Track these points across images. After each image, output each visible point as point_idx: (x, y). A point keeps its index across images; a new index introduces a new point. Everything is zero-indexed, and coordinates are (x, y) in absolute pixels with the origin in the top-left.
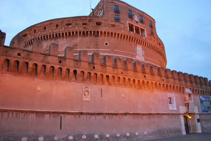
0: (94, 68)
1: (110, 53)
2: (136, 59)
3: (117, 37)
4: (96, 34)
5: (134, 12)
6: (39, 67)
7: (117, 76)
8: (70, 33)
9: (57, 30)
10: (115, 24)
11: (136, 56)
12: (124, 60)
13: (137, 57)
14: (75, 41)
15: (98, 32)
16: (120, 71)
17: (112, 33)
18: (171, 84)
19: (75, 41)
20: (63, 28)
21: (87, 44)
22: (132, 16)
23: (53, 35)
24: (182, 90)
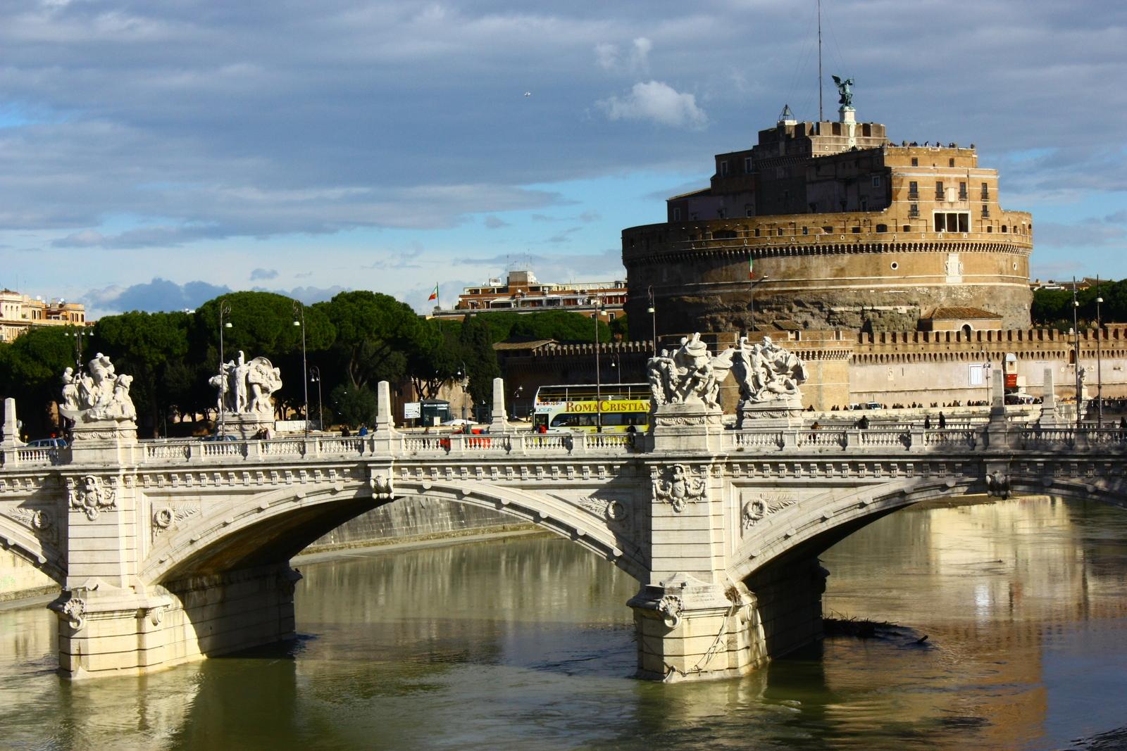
2: (945, 284)
4: (877, 248)
6: (857, 357)
14: (840, 261)
16: (921, 346)
17: (904, 245)
21: (861, 267)
23: (799, 248)
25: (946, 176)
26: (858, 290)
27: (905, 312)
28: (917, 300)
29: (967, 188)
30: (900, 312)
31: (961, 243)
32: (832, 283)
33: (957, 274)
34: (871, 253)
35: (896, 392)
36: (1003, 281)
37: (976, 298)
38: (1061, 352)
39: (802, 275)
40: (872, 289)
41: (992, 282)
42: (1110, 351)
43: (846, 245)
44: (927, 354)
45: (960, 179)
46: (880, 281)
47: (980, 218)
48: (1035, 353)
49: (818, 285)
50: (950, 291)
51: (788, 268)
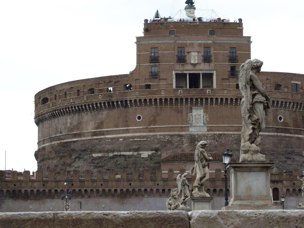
1: (143, 132)
2: (188, 133)
3: (154, 104)
4: (125, 104)
5: (189, 46)
7: (96, 189)
8: (93, 104)
10: (151, 84)
11: (190, 128)
12: (165, 139)
13: (191, 129)
14: (100, 116)
15: (126, 101)
17: (145, 100)
19: (101, 116)
20: (85, 97)
21: (115, 120)
22: (186, 56)
25: (188, 42)
26: (112, 139)
27: (147, 156)
28: (158, 146)
29: (212, 52)
30: (142, 156)
32: (95, 134)
33: (202, 125)
34: (121, 109)
37: (222, 145)
39: (78, 129)
40: (121, 138)
43: (102, 102)
44: (107, 190)
45: (204, 44)
46: (127, 131)
47: (227, 77)
49: (87, 137)
51: (71, 123)
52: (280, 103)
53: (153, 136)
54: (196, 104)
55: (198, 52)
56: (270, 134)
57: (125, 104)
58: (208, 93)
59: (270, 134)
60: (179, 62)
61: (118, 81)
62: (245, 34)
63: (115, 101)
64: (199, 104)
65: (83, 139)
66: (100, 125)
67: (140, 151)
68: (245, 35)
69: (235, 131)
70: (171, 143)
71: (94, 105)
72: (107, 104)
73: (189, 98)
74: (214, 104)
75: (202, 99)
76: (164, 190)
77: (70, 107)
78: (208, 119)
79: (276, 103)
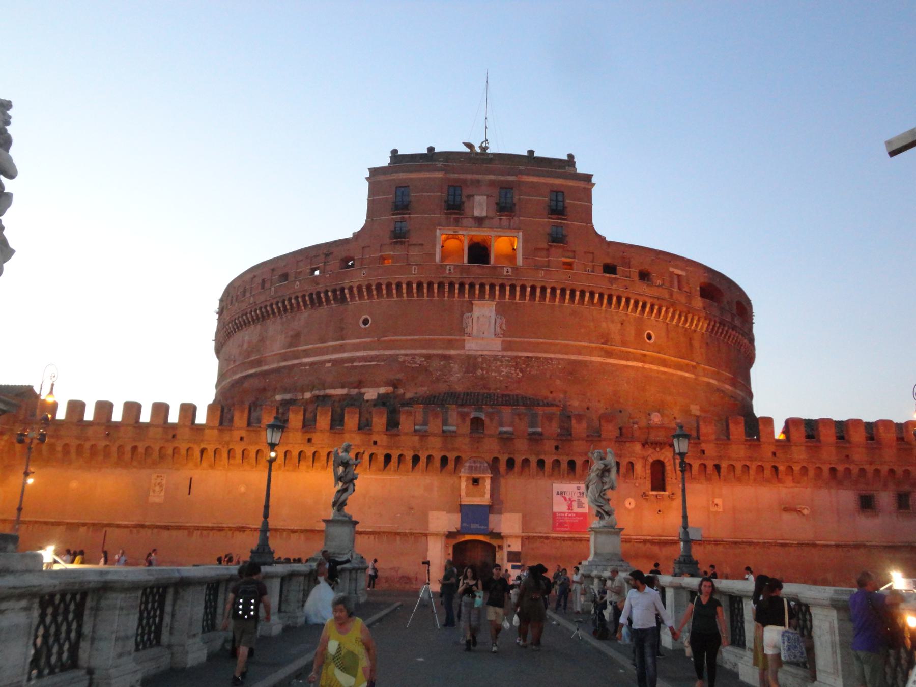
0: (174, 436)
1: (370, 349)
2: (461, 352)
4: (340, 296)
9: (262, 298)
13: (468, 345)
15: (342, 290)
18: (405, 453)
20: (273, 289)
24: (451, 465)
25: (469, 176)
26: (312, 364)
28: (400, 376)
30: (366, 397)
31: (498, 283)
32: (285, 357)
35: (167, 528)
36: (609, 354)
38: (624, 462)
40: (329, 361)
41: (580, 354)
42: (768, 466)
43: (300, 294)
45: (502, 182)
46: (342, 349)
48: (549, 461)
50: (471, 363)
51: (249, 343)
52: (648, 306)
53: (391, 356)
54: (482, 297)
55: (488, 196)
56: (630, 363)
57: (340, 296)
58: (505, 273)
59: (630, 363)
60: (451, 214)
61: (331, 253)
62: (581, 168)
63: (323, 289)
64: (487, 296)
65: (265, 368)
66: (296, 338)
67: (364, 387)
68: (578, 171)
69: (559, 352)
70: (427, 370)
71: (286, 303)
72: (307, 298)
73: (467, 281)
74: (517, 297)
75: (492, 286)
76: (388, 458)
77: (249, 311)
78: (504, 327)
79: (641, 304)
